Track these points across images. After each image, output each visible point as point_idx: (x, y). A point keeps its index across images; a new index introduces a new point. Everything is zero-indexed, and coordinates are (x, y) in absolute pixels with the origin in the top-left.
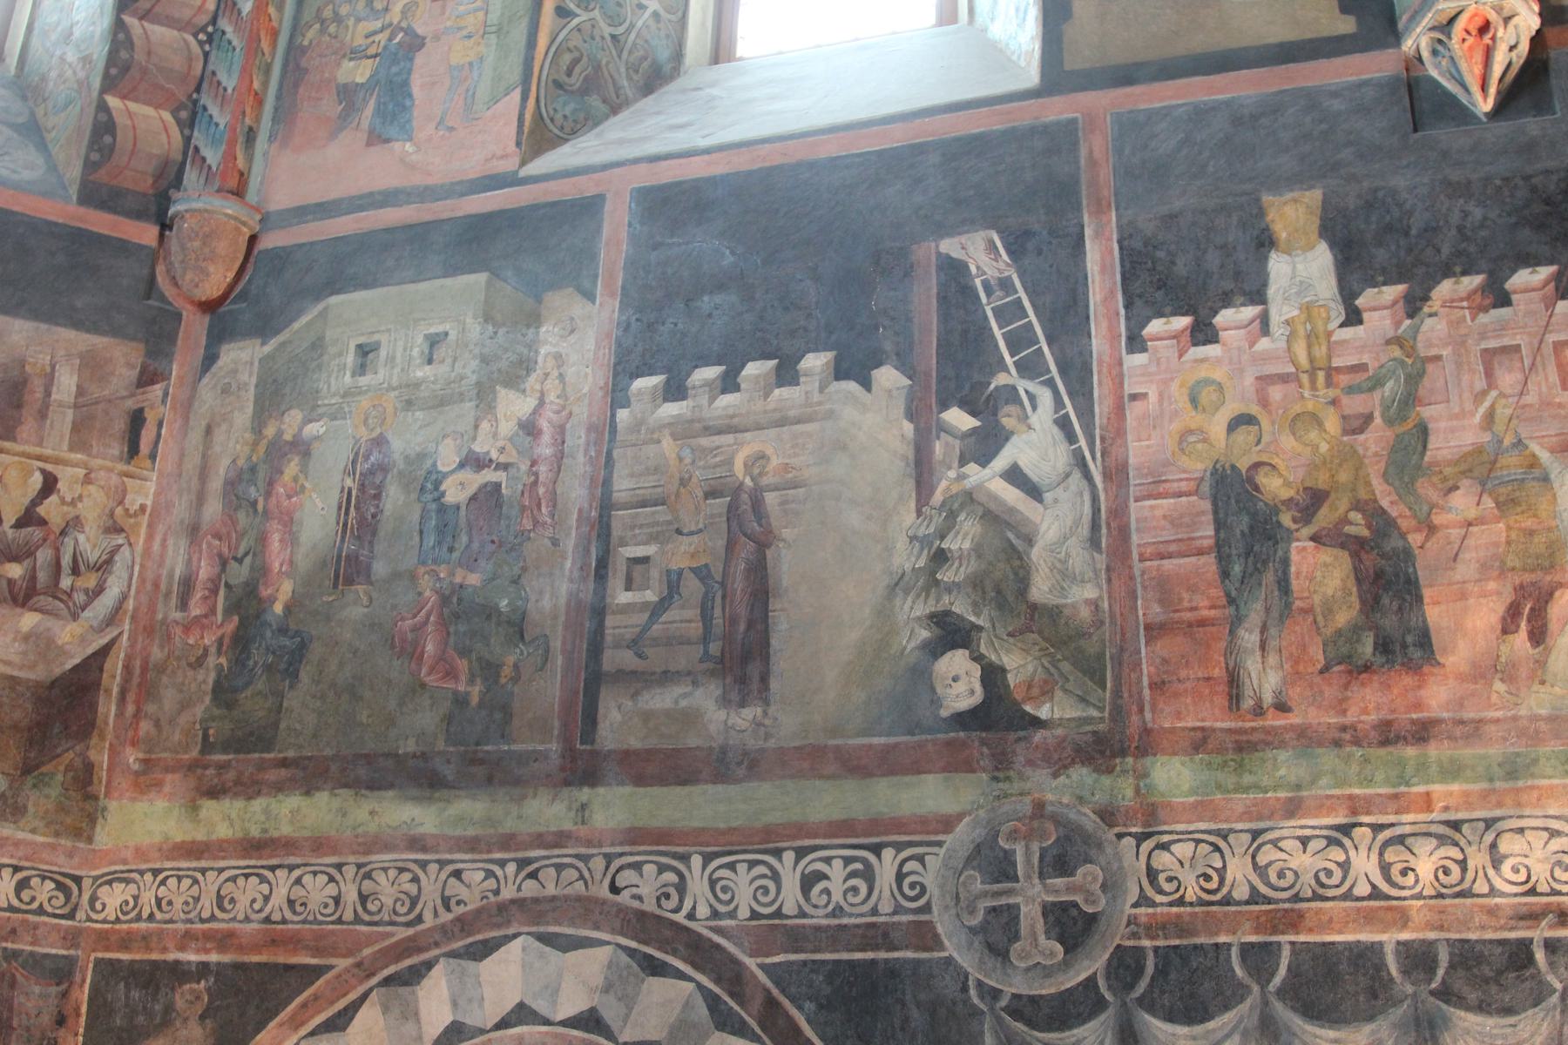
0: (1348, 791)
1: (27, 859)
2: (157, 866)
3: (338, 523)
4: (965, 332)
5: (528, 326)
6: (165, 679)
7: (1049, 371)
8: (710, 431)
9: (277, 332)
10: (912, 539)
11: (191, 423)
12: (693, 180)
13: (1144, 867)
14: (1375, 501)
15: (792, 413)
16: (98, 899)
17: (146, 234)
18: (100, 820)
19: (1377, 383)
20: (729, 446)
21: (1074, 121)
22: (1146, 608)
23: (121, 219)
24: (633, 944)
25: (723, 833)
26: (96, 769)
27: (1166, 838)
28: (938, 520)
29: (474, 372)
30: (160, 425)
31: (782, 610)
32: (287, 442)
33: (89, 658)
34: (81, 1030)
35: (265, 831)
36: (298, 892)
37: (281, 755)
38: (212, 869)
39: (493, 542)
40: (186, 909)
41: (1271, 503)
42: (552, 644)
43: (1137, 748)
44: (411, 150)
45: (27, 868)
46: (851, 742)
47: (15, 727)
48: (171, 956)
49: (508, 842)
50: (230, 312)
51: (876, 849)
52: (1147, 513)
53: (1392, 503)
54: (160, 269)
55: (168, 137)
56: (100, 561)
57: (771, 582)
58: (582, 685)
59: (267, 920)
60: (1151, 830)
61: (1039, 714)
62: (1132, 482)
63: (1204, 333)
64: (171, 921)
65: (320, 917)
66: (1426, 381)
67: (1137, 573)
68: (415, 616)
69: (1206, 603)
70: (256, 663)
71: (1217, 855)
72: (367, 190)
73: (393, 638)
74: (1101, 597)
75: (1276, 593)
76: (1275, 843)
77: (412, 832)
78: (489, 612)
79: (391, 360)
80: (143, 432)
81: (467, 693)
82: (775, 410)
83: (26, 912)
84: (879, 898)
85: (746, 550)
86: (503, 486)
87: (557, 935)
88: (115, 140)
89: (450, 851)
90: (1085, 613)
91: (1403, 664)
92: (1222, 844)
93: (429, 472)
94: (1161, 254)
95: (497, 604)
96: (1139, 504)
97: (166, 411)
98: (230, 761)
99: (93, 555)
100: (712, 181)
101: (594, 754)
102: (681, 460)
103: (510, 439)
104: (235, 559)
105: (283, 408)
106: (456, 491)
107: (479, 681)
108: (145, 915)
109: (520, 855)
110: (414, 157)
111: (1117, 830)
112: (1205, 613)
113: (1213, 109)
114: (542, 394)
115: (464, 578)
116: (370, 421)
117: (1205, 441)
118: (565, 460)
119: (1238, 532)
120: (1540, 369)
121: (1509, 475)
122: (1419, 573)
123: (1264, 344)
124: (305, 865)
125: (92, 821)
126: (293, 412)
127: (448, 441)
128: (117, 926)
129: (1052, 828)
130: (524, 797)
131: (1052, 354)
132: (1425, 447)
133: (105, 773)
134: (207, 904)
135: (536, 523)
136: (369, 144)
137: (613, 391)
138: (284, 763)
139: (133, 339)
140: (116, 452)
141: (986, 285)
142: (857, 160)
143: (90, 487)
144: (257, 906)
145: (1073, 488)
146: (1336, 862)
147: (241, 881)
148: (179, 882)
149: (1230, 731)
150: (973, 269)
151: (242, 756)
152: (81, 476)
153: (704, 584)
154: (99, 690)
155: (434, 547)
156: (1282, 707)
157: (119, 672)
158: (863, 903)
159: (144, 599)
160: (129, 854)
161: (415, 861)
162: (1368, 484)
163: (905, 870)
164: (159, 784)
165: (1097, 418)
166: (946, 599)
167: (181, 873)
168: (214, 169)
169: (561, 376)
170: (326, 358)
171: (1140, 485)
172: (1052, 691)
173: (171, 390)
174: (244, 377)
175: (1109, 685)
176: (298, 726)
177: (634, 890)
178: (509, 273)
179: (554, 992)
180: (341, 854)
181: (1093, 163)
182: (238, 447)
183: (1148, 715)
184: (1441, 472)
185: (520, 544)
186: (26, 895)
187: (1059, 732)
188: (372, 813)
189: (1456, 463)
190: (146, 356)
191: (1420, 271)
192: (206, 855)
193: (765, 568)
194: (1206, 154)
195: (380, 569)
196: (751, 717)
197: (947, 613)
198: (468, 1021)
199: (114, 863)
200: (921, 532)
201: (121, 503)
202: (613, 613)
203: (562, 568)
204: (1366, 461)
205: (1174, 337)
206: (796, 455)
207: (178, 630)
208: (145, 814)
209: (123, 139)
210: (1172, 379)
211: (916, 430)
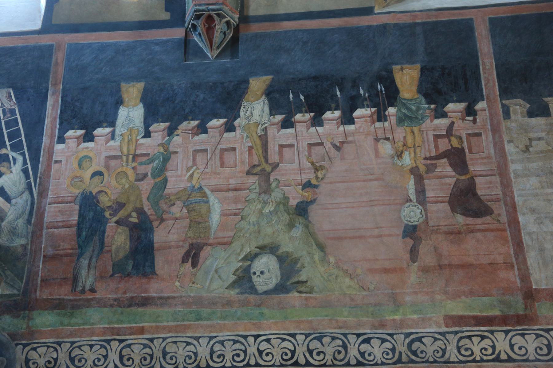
0: (112, 326)
7: (23, 149)
13: (24, 358)
14: (143, 208)
19: (152, 161)
21: (52, 46)
22: (44, 248)
27: (35, 345)
41: (102, 207)
43: (31, 307)
53: (149, 209)
60: (30, 342)
62: (49, 196)
63: (89, 137)
66: (170, 161)
67: (44, 233)
69: (70, 247)
71: (55, 353)
74: (28, 244)
75: (98, 244)
76: (79, 347)
90: (20, 250)
91: (142, 274)
92: (58, 348)
94: (77, 104)
96: (50, 205)
111: (16, 342)
113: (109, 46)
119: (88, 219)
120: (213, 159)
121: (194, 200)
122: (154, 237)
123: (112, 143)
132: (165, 188)
146: (103, 355)
149: (70, 300)
156: (93, 290)
162: (141, 201)
171: (52, 198)
175: (24, 280)
181: (57, 64)
183: (38, 293)
184: (169, 198)
189: (176, 194)
191: (176, 118)
194: (102, 64)
204: (142, 192)
205: (77, 138)
210: (73, 155)
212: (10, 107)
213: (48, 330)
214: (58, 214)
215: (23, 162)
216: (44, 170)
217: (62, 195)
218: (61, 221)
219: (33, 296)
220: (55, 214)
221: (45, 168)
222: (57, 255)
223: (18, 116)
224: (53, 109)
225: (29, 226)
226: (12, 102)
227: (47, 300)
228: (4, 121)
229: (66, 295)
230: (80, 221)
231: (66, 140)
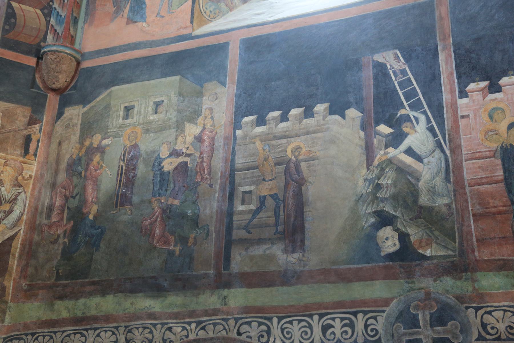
3: (117, 181)
4: (386, 93)
5: (198, 97)
6: (40, 250)
7: (423, 107)
8: (276, 138)
9: (90, 102)
10: (366, 180)
11: (52, 141)
12: (267, 35)
13: (480, 322)
15: (311, 129)
17: (32, 61)
20: (285, 144)
22: (472, 206)
23: (19, 54)
25: (286, 307)
26: (7, 289)
27: (489, 309)
28: (376, 171)
29: (175, 117)
30: (38, 141)
31: (310, 211)
32: (94, 147)
33: (5, 240)
35: (83, 313)
37: (92, 280)
38: (59, 331)
39: (184, 186)
42: (210, 228)
43: (472, 268)
44: (145, 26)
46: (341, 267)
49: (192, 314)
50: (69, 94)
51: (355, 314)
52: (471, 166)
54: (37, 76)
55: (39, 20)
56: (11, 199)
57: (304, 200)
58: (224, 245)
60: (482, 305)
61: (426, 254)
62: (463, 153)
63: (495, 88)
67: (468, 192)
68: (151, 218)
69: (501, 204)
70: (81, 241)
72: (127, 43)
73: (142, 228)
74: (452, 203)
77: (149, 311)
78: (183, 216)
79: (139, 113)
80: (31, 144)
81: (174, 251)
82: (304, 128)
84: (357, 336)
85: (293, 186)
86: (188, 163)
88: (16, 21)
89: (167, 319)
90: (444, 210)
93: (156, 158)
94: (473, 55)
95: (186, 212)
96: (467, 162)
97: (41, 136)
98: (69, 283)
99: (8, 197)
100: (274, 35)
101: (230, 274)
102: (264, 150)
103: (191, 144)
104: (72, 197)
105: (93, 133)
106: (168, 165)
107: (179, 245)
109: (197, 320)
110: (147, 29)
111: (465, 305)
112: (501, 208)
114: (204, 125)
115: (172, 202)
116: (131, 138)
117: (497, 134)
118: (215, 152)
124: (102, 328)
126: (97, 135)
127: (165, 145)
129: (435, 304)
130: (199, 294)
131: (425, 100)
133: (11, 291)
135: (203, 178)
136: (128, 23)
137: (235, 123)
138: (93, 283)
139: (26, 105)
140: (18, 152)
141: (394, 73)
142: (336, 23)
143: (7, 167)
145: (436, 156)
147: (72, 336)
148: (44, 338)
150: (389, 67)
151: (74, 281)
152: (3, 163)
153: (275, 201)
154: (9, 254)
155: (159, 189)
157: (19, 246)
158: (350, 338)
161: (151, 324)
163: (368, 323)
164: (36, 295)
165: (446, 127)
166: (381, 205)
167: (44, 334)
168: (60, 34)
169: (212, 118)
170: (111, 112)
171: (467, 154)
172: (431, 244)
173: (43, 127)
174: (75, 121)
175: (457, 241)
176: (99, 267)
177: (248, 334)
178: (189, 76)
181: (441, 18)
182: (73, 150)
183: (477, 254)
185: (196, 187)
187: (435, 261)
188: (132, 303)
190: (32, 112)
193: (302, 194)
194: (493, 11)
195: (135, 199)
196: (297, 257)
197: (382, 211)
199: (14, 331)
200: (369, 177)
201: (21, 174)
202: (237, 214)
203: (214, 196)
206: (313, 147)
207: (46, 228)
208: (29, 308)
209: (20, 20)
210: (480, 108)
211: (366, 134)
212: (400, 68)
213: (499, 293)
214: (479, 170)
215: (426, 121)
216: (452, 126)
217: (478, 151)
218: (484, 178)
219: (471, 256)
220: (475, 170)
221: (452, 124)
222: (487, 213)
223: (410, 75)
224: (446, 64)
225: (448, 185)
226: (401, 63)
227: (489, 261)
228: (398, 82)
229: (509, 255)
230: (507, 176)
231: (469, 94)
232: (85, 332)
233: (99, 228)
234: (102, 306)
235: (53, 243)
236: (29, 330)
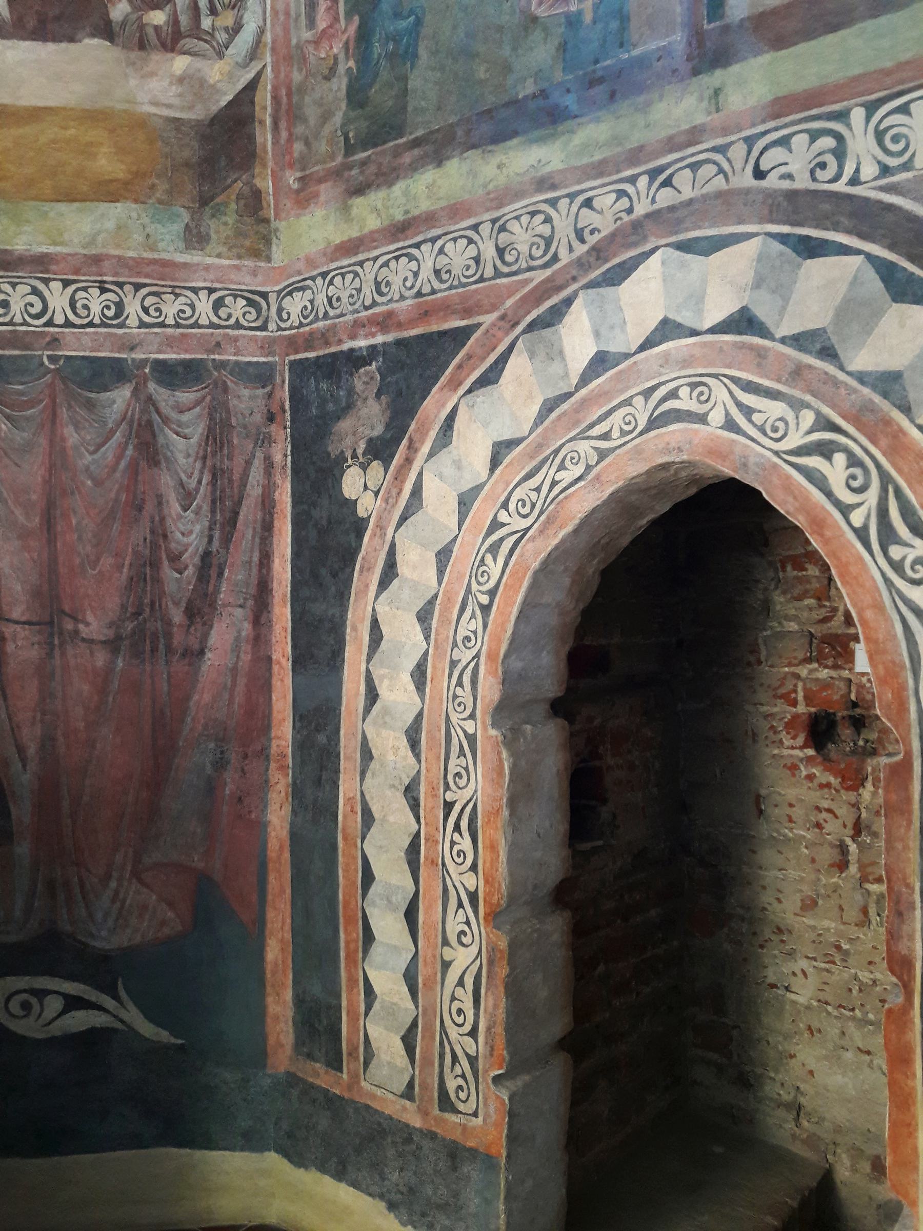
1: (218, 281)
2: (325, 269)
16: (283, 309)
18: (274, 240)
24: (785, 229)
25: (887, 73)
33: (240, 93)
34: (288, 423)
36: (442, 261)
37: (413, 136)
38: (368, 260)
40: (352, 301)
45: (220, 289)
47: (187, 164)
48: (345, 347)
49: (635, 156)
59: (419, 294)
64: (342, 315)
65: (464, 280)
70: (380, 55)
77: (540, 174)
81: (580, 13)
83: (226, 327)
87: (697, 239)
89: (579, 182)
98: (369, 156)
101: (726, 29)
108: (321, 315)
109: (651, 165)
124: (446, 234)
125: (267, 241)
128: (301, 330)
130: (649, 104)
133: (271, 197)
134: (368, 293)
138: (416, 143)
144: (408, 284)
147: (393, 264)
151: (379, 148)
154: (254, 121)
157: (269, 102)
159: (279, 30)
160: (301, 265)
161: (545, 201)
164: (316, 195)
177: (783, 170)
179: (698, 299)
180: (476, 215)
186: (223, 312)
188: (500, 167)
192: (361, 249)
198: (612, 349)
207: (311, 48)
208: (309, 226)
232: (414, 251)
233: (411, 12)
234: (440, 187)
235: (327, 78)
236: (316, 268)
